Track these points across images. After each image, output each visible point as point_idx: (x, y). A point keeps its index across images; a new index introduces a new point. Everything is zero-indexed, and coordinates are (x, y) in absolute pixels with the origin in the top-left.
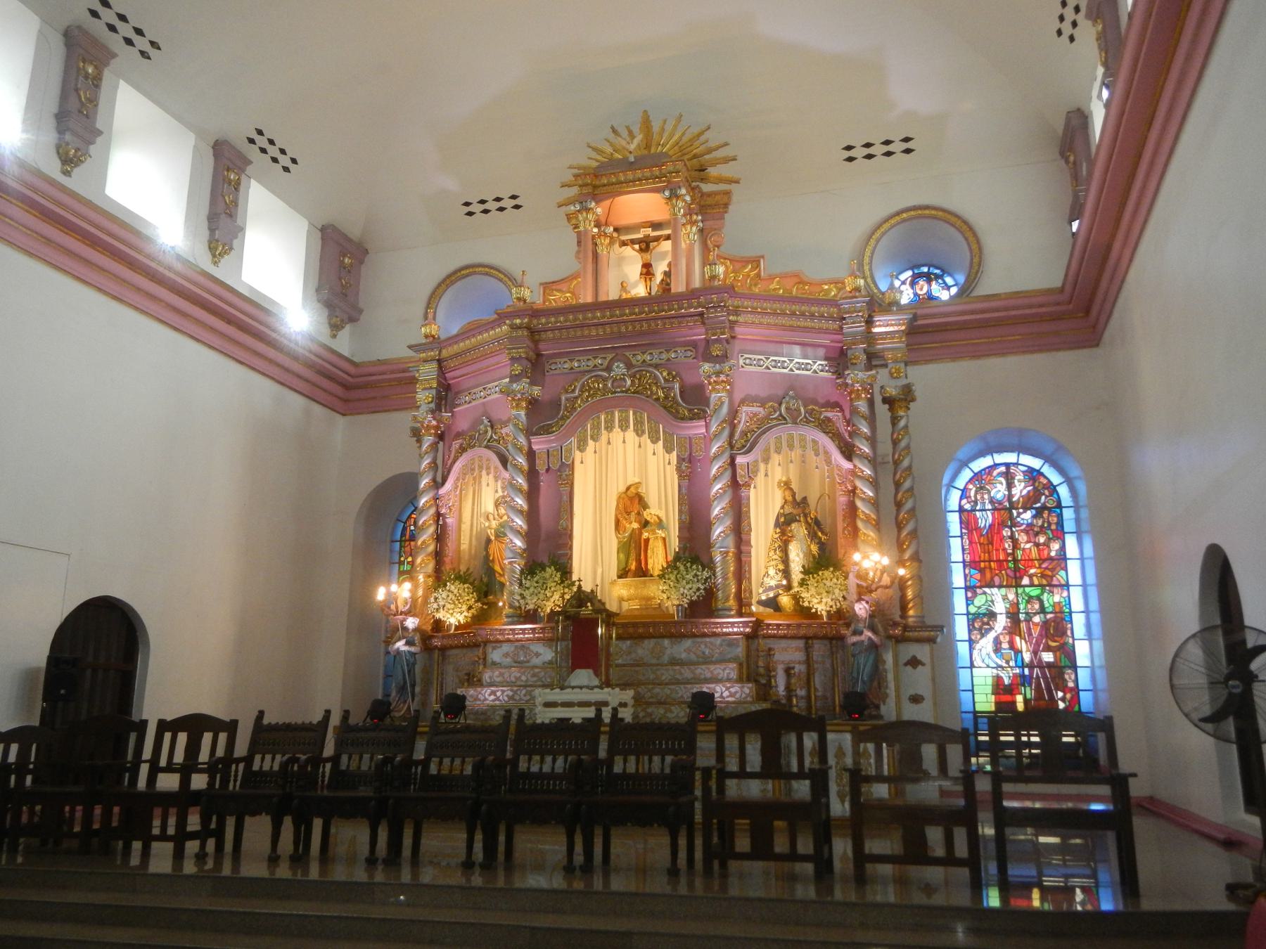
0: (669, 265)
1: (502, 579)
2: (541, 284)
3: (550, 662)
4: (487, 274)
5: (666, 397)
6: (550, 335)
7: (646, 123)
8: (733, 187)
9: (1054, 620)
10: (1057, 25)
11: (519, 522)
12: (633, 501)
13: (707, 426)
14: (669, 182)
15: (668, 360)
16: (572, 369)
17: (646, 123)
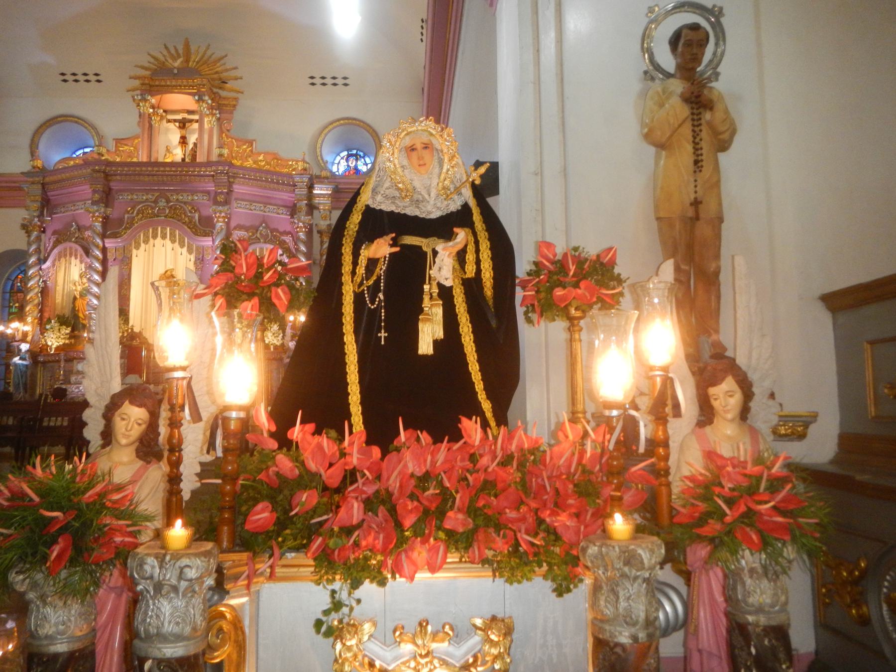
0: (197, 140)
1: (84, 322)
2: (114, 139)
4: (76, 122)
5: (190, 222)
6: (118, 178)
7: (187, 45)
8: (239, 95)
10: (420, 37)
13: (213, 241)
14: (199, 91)
15: (193, 200)
16: (132, 199)
17: (187, 45)
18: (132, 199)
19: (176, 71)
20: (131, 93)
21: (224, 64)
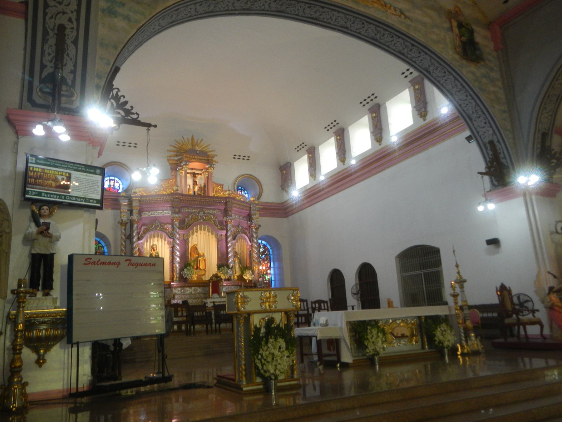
3: (191, 293)
4: (121, 166)
9: (268, 282)
11: (178, 253)
12: (195, 248)
18: (188, 211)
19: (198, 152)
20: (169, 158)
21: (209, 149)
